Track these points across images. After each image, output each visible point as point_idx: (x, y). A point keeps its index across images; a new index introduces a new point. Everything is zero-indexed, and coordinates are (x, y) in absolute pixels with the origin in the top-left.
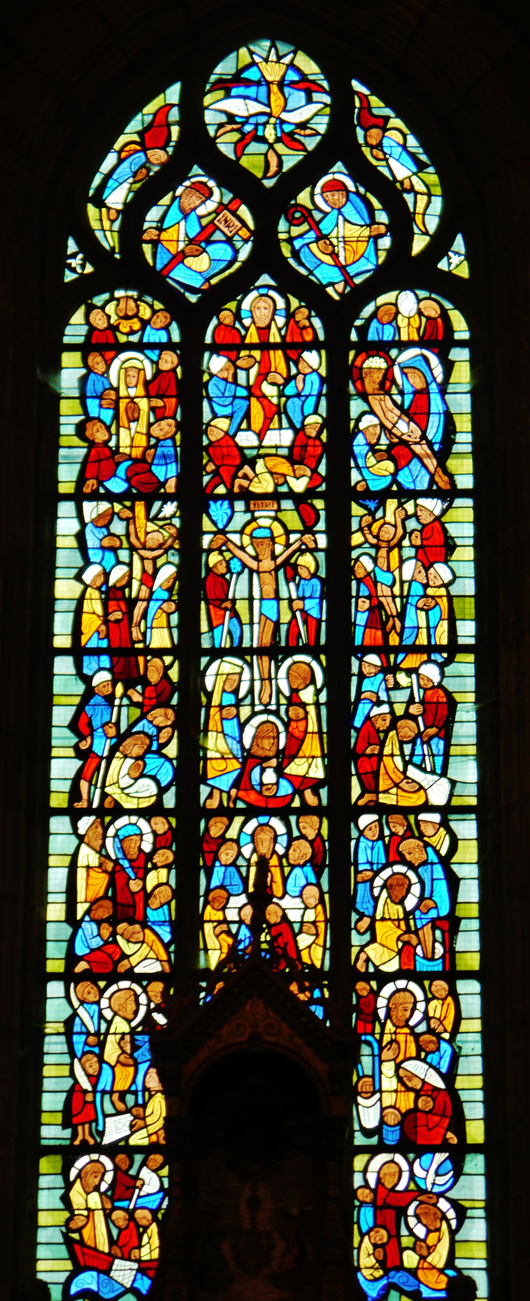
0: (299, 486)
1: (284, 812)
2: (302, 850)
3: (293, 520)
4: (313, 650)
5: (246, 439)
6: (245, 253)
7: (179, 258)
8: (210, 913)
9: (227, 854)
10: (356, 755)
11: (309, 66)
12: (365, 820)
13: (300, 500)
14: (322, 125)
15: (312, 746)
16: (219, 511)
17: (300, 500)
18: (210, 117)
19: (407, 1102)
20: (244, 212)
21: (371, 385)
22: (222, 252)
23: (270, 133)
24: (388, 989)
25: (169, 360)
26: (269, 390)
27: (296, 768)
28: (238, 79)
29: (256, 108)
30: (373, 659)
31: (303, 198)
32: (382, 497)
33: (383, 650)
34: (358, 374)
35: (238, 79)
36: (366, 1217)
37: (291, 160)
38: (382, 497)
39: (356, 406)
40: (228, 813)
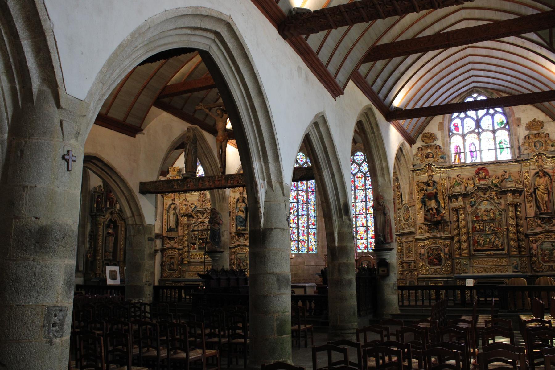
0: (363, 188)
1: (362, 214)
2: (364, 217)
3: (362, 191)
4: (364, 201)
5: (359, 185)
6: (358, 170)
7: (353, 171)
8: (357, 222)
9: (358, 218)
10: (368, 210)
11: (362, 154)
12: (368, 214)
13: (363, 190)
14: (363, 159)
15: (364, 209)
16: (357, 191)
17: (363, 190)
18: (355, 159)
19: (372, 235)
20: (358, 166)
21: (368, 180)
22: (356, 170)
23: (359, 160)
24: (370, 227)
25: (353, 179)
26: (360, 181)
27: (363, 211)
28: (357, 156)
29: (358, 158)
30: (368, 202)
31: (362, 165)
32: (369, 189)
33: (369, 201)
34: (366, 179)
35: (357, 156)
36: (369, 244)
37: (361, 162)
38: (369, 189)
39: (367, 182)
40: (358, 215)
